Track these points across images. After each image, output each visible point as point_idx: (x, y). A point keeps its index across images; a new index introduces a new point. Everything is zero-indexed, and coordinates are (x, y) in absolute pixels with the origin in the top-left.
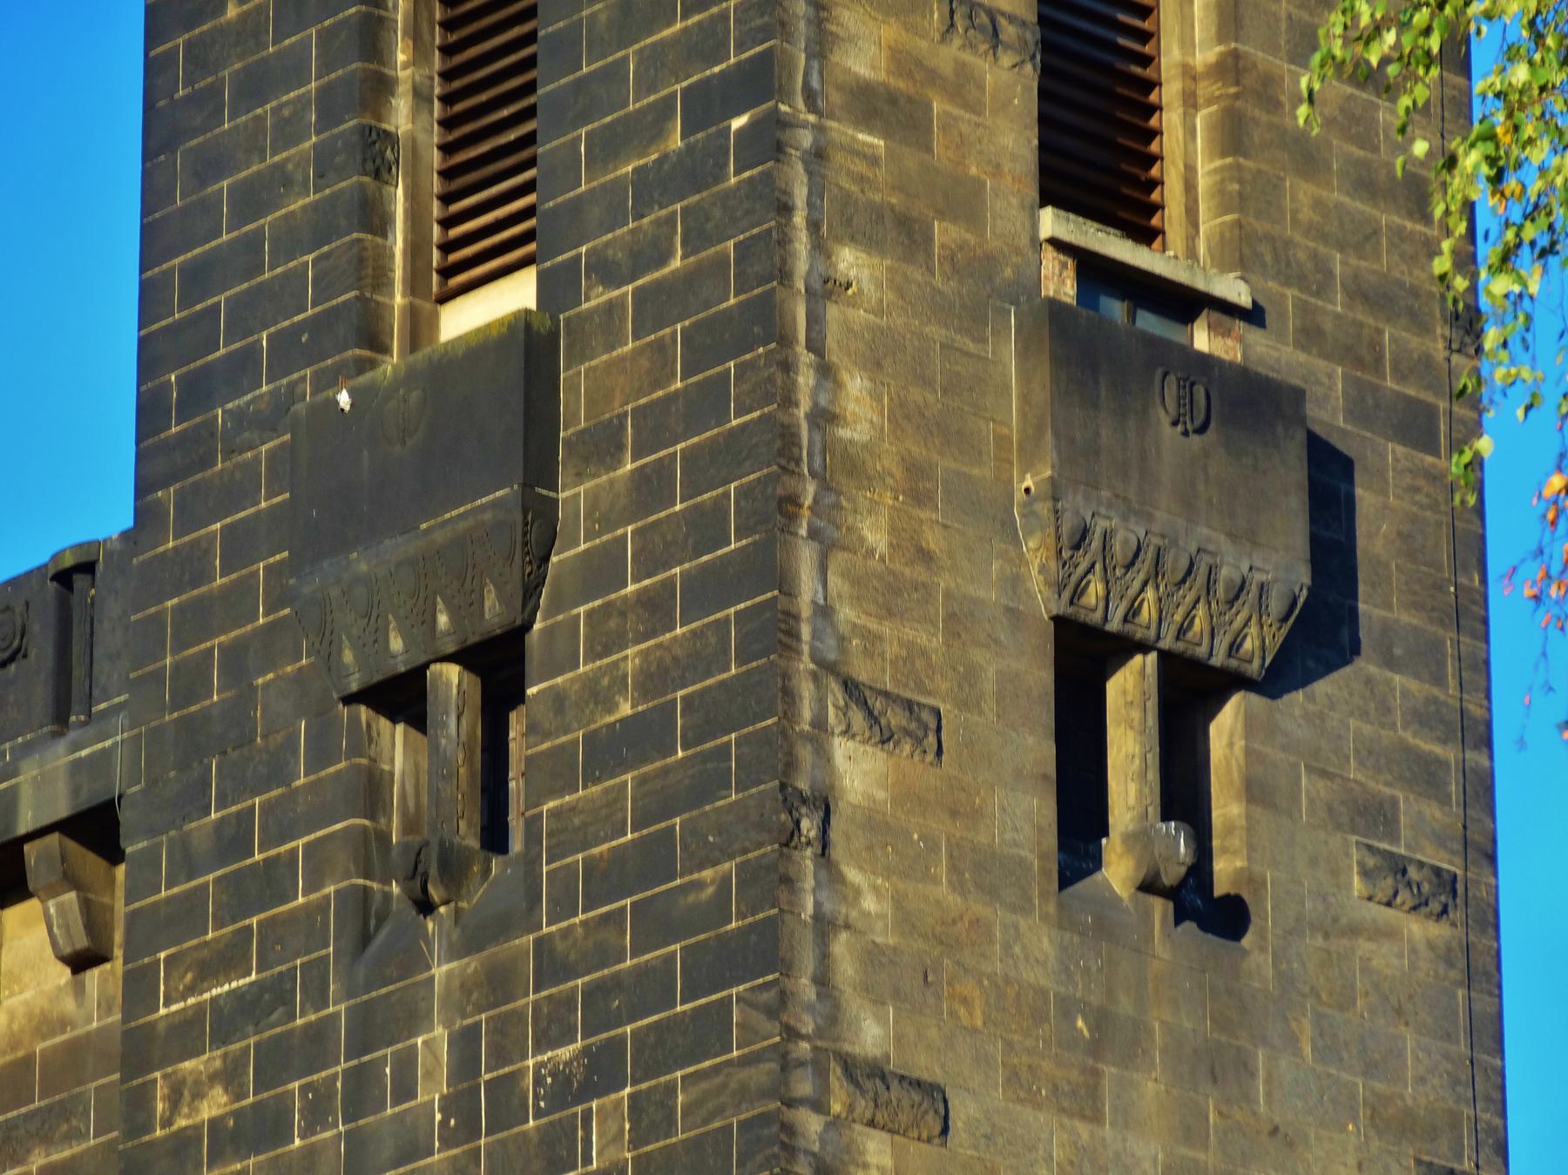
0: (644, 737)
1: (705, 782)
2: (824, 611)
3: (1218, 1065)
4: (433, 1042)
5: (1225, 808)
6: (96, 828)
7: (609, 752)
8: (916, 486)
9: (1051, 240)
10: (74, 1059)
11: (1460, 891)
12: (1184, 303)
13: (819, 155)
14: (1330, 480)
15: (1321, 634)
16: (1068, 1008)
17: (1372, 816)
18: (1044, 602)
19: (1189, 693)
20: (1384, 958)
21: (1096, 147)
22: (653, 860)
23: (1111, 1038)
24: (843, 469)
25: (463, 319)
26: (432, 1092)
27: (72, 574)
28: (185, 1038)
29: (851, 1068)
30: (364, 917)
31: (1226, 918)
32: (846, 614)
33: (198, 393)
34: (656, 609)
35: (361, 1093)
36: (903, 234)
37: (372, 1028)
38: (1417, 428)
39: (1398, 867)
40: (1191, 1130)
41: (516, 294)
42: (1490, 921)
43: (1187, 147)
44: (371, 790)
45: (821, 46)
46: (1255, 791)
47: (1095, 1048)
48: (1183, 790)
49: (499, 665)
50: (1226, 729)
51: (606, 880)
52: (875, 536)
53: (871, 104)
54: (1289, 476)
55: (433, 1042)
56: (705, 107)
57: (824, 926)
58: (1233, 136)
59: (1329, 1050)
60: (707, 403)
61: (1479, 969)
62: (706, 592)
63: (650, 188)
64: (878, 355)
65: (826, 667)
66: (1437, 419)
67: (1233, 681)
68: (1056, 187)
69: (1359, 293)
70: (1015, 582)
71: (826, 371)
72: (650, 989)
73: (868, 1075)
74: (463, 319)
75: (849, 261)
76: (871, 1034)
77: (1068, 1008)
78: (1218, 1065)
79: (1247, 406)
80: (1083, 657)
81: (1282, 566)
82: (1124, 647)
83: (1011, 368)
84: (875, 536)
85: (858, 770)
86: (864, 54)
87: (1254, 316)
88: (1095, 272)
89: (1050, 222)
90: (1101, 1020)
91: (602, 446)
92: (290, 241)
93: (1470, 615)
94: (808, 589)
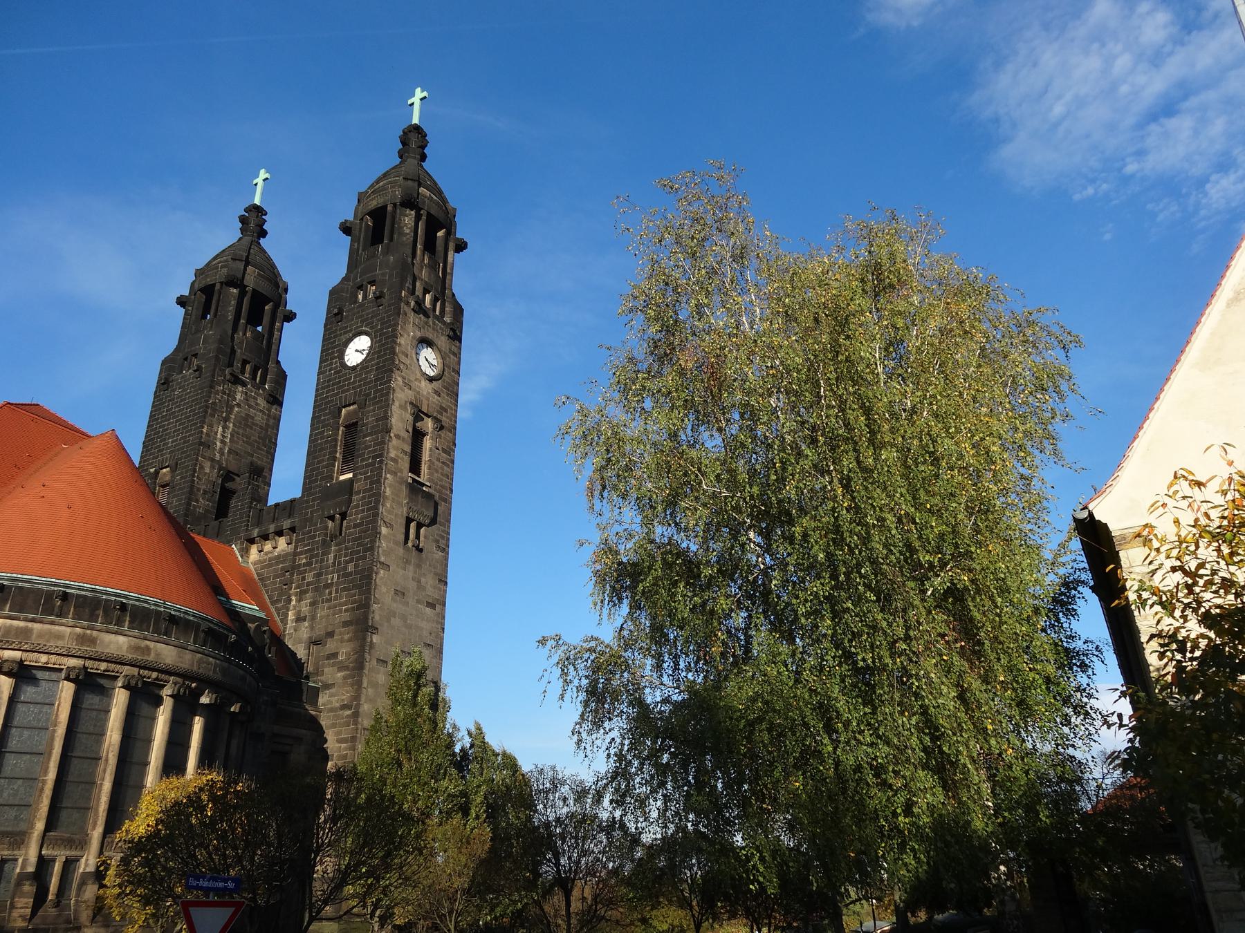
0: (360, 524)
1: (367, 530)
3: (419, 566)
5: (422, 538)
6: (293, 529)
7: (356, 526)
10: (286, 555)
11: (445, 550)
12: (423, 485)
14: (436, 505)
15: (433, 521)
17: (437, 541)
19: (419, 526)
21: (415, 467)
22: (360, 538)
23: (408, 562)
24: (386, 498)
25: (342, 478)
26: (331, 561)
27: (293, 501)
28: (301, 553)
30: (324, 541)
31: (421, 550)
33: (310, 483)
34: (363, 511)
35: (322, 561)
36: (394, 474)
37: (324, 554)
38: (445, 501)
41: (350, 475)
43: (424, 469)
44: (326, 528)
48: (418, 536)
49: (344, 516)
50: (422, 530)
51: (354, 540)
54: (432, 504)
56: (374, 458)
58: (429, 468)
61: (446, 559)
62: (368, 510)
63: (367, 466)
66: (448, 501)
68: (411, 471)
72: (358, 552)
73: (382, 563)
74: (342, 478)
76: (382, 559)
78: (419, 566)
79: (429, 496)
80: (409, 521)
81: (431, 514)
83: (404, 490)
85: (384, 530)
91: (358, 493)
92: (324, 467)
93: (449, 521)
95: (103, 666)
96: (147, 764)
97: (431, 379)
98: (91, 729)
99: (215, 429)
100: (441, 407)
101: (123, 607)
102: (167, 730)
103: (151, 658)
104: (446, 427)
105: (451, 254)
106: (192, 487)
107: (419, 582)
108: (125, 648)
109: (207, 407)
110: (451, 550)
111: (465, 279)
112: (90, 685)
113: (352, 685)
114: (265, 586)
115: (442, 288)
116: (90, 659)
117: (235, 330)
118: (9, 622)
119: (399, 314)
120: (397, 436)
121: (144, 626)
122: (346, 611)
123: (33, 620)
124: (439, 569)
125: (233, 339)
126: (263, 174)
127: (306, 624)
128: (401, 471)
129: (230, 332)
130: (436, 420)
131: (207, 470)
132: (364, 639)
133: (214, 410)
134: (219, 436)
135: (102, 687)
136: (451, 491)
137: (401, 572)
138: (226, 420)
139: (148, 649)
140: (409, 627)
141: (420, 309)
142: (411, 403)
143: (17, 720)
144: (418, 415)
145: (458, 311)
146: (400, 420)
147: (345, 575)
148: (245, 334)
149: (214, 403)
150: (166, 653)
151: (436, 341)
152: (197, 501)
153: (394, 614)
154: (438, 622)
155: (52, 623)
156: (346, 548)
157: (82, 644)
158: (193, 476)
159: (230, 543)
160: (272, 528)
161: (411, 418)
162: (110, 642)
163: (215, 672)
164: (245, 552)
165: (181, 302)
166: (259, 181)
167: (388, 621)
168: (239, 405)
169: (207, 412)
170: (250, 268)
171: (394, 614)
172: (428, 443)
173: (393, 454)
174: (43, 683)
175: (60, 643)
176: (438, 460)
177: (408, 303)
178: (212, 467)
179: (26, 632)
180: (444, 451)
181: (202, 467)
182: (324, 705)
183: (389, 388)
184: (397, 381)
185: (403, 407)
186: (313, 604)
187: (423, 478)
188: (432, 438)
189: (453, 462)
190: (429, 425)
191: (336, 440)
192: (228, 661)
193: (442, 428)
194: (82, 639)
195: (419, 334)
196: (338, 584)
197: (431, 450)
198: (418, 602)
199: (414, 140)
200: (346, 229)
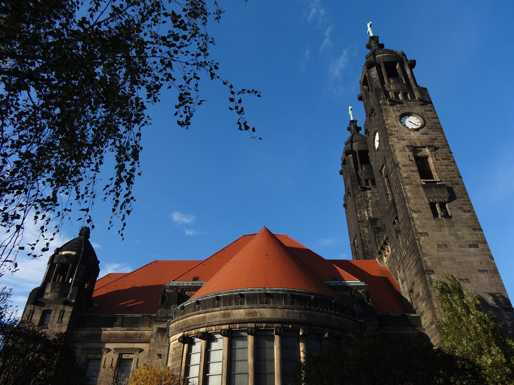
2: (409, 207)
3: (452, 226)
4: (401, 242)
8: (415, 198)
9: (423, 182)
11: (471, 210)
13: (402, 182)
15: (452, 197)
16: (437, 226)
17: (461, 208)
18: (428, 202)
20: (465, 216)
22: (405, 226)
24: (408, 199)
29: (419, 233)
31: (451, 217)
32: (411, 206)
36: (411, 184)
38: (458, 184)
39: (464, 211)
40: (450, 231)
42: (474, 212)
45: (401, 176)
46: (450, 209)
47: (440, 227)
52: (413, 201)
53: (405, 178)
55: (401, 242)
56: (396, 182)
57: (414, 225)
58: (437, 172)
59: (461, 223)
60: (400, 198)
64: (410, 191)
65: (410, 210)
67: (445, 203)
68: (422, 178)
69: (449, 178)
70: (425, 201)
71: (406, 193)
73: (421, 233)
75: (406, 187)
76: (420, 231)
77: (437, 226)
78: (452, 226)
80: (432, 206)
81: (446, 194)
82: (435, 203)
83: (421, 189)
84: (413, 201)
85: (414, 215)
86: (404, 175)
87: (441, 181)
88: (426, 182)
89: (422, 180)
90: (440, 226)
93: (466, 194)
94: (408, 206)
95: (238, 326)
96: (274, 374)
97: (417, 130)
98: (242, 359)
99: (363, 213)
100: (431, 139)
101: (242, 296)
102: (278, 353)
103: (258, 316)
104: (441, 147)
105: (408, 72)
106: (362, 242)
107: (456, 235)
108: (244, 315)
109: (356, 206)
110: (475, 209)
111: (421, 76)
112: (232, 336)
113: (430, 309)
114: (392, 272)
115: (409, 87)
116: (231, 324)
117: (357, 169)
118: (199, 315)
119: (381, 111)
120: (405, 166)
121: (255, 302)
122: (414, 267)
123: (206, 312)
124: (470, 223)
125: (357, 174)
126: (350, 108)
127: (405, 283)
128: (415, 181)
129: (355, 172)
130: (429, 147)
131: (367, 232)
132: (425, 279)
133: (360, 206)
134: (366, 215)
135: (243, 336)
136: (461, 177)
137: (439, 234)
138: (367, 207)
139: (255, 312)
140: (460, 263)
141: (393, 103)
142: (407, 146)
143: (212, 359)
144: (415, 149)
145: (423, 91)
146: (403, 157)
147: (408, 248)
148: (362, 169)
149: (358, 203)
150: (266, 312)
151: (413, 111)
152: (367, 247)
153: (443, 259)
154: (484, 255)
155: (212, 311)
156: (403, 234)
157: (225, 318)
158: (361, 237)
159: (373, 258)
160: (382, 243)
161: (411, 154)
162: (237, 314)
163: (300, 317)
164: (381, 259)
165: (341, 173)
166: (350, 112)
167: (440, 264)
168: (370, 199)
169: (357, 207)
170: (354, 144)
171: (443, 259)
172: (431, 160)
173: (404, 175)
174: (219, 340)
175: (216, 320)
176: (441, 165)
177: (385, 104)
178: (368, 229)
179: (204, 318)
180: (443, 159)
181: (363, 232)
182: (424, 326)
183: (390, 145)
184: (393, 140)
185: (403, 150)
186: (404, 271)
187: (436, 178)
188: (432, 157)
189: (454, 162)
190: (427, 151)
191: (385, 186)
192: (306, 309)
193: (436, 149)
194: (225, 315)
195: (399, 114)
196: (407, 254)
197: (433, 163)
198: (460, 247)
199: (375, 44)
200: (360, 98)
